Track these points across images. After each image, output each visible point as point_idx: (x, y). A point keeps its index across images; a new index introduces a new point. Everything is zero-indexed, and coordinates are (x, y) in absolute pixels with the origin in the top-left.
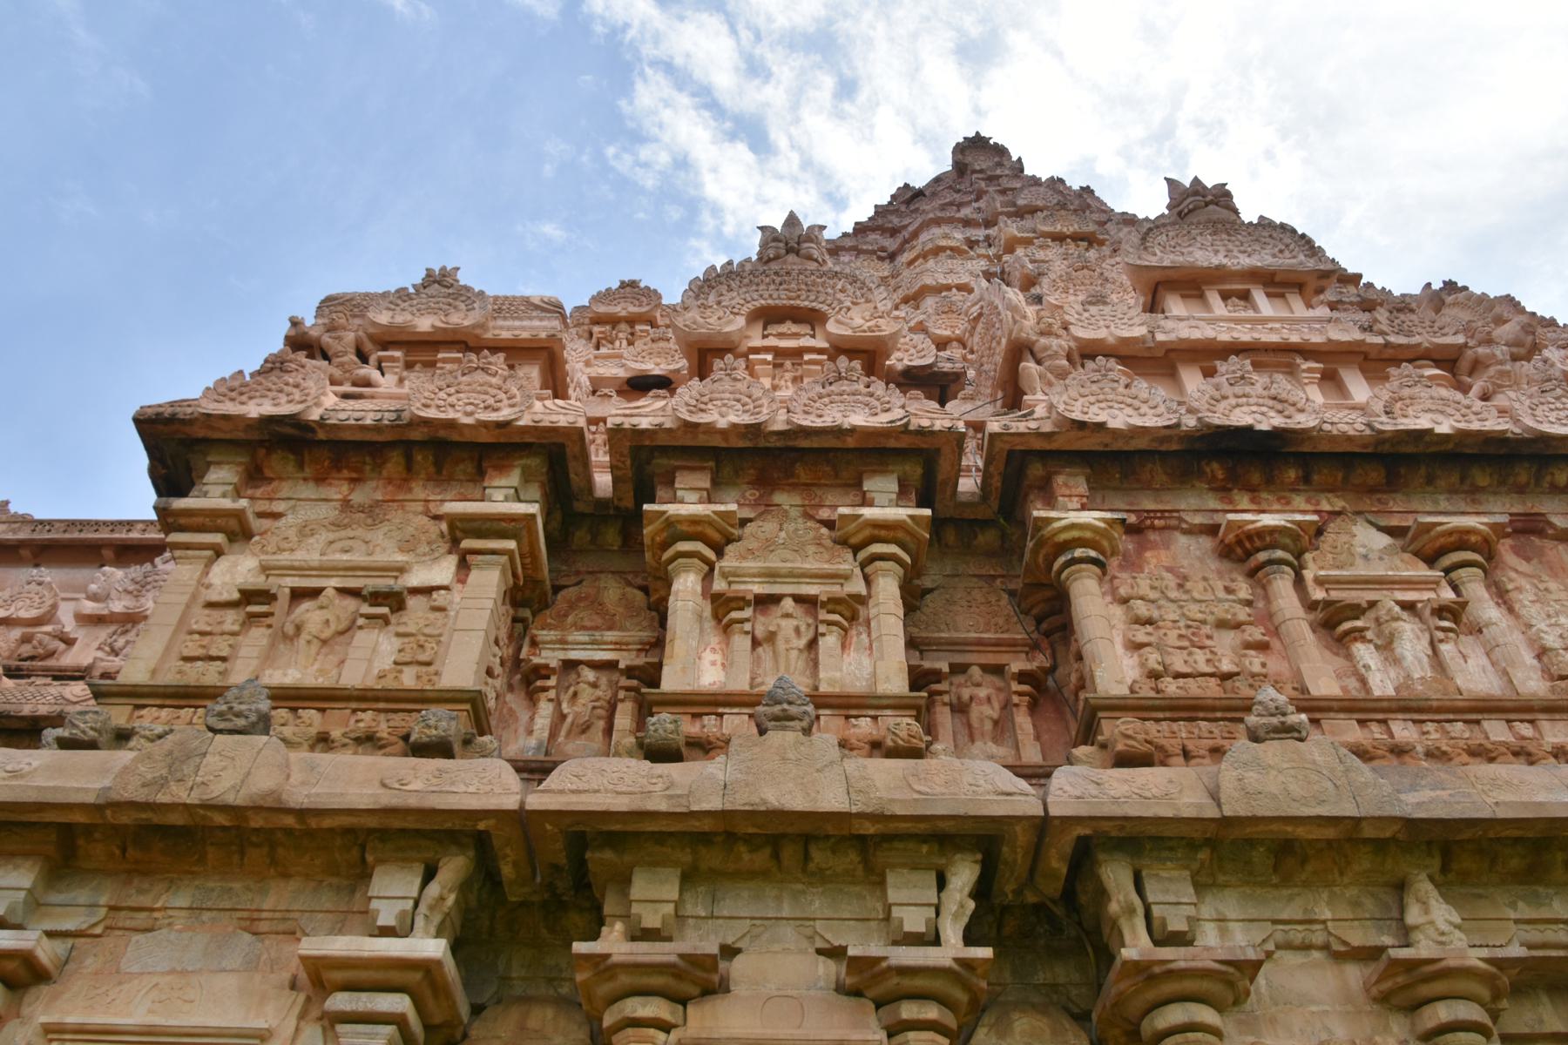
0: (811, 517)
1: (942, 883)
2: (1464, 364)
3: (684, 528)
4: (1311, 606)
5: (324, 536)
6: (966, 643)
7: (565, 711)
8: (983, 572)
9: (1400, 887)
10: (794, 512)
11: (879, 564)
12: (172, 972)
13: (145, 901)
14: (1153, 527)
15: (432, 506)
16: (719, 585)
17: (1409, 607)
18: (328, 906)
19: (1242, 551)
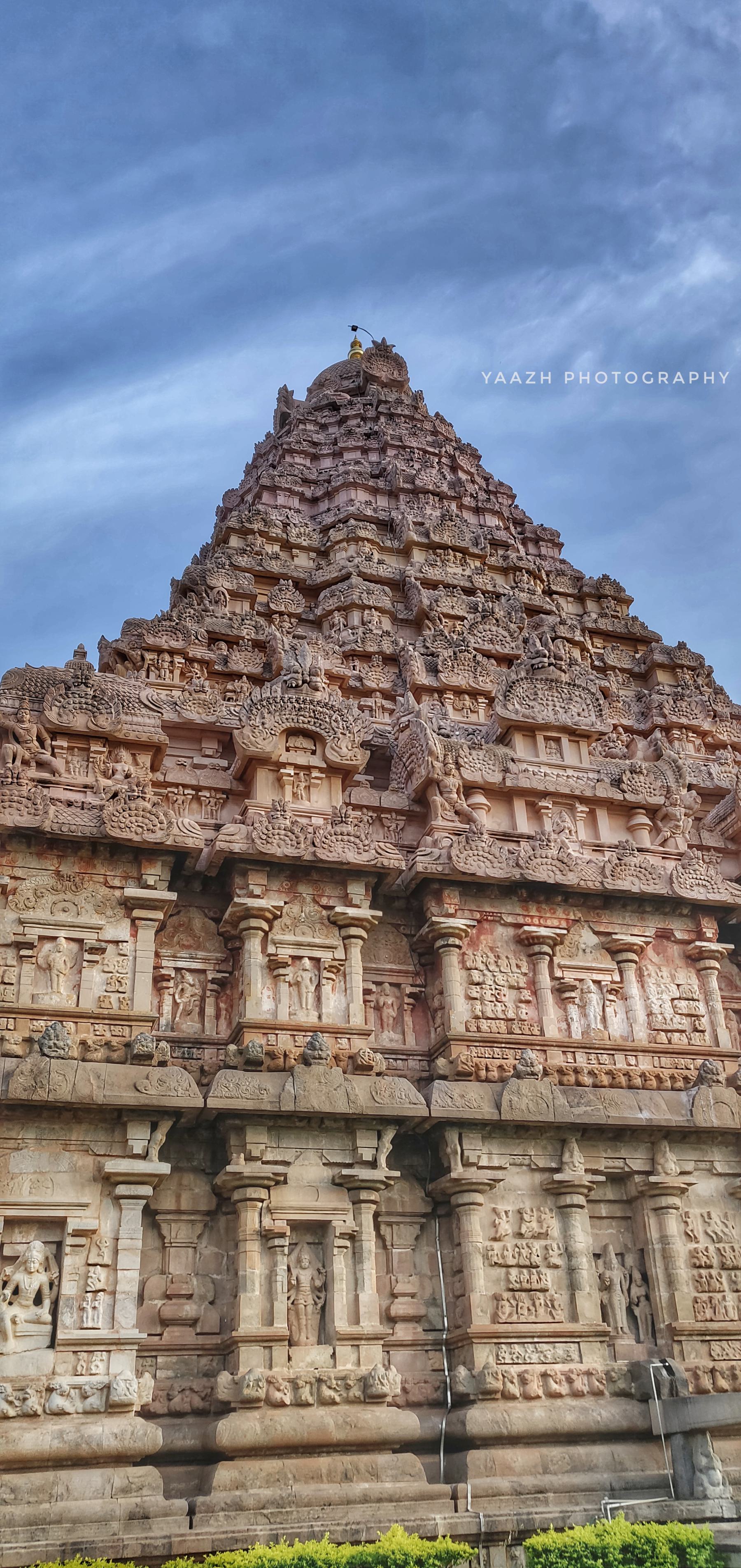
0: (317, 903)
1: (379, 1137)
2: (660, 814)
3: (255, 912)
4: (553, 978)
5: (50, 898)
6: (384, 970)
7: (178, 1001)
8: (394, 921)
9: (564, 1142)
10: (308, 899)
11: (353, 940)
12: (35, 1172)
13: (13, 1134)
14: (487, 920)
15: (109, 878)
16: (271, 949)
17: (597, 982)
18: (103, 1139)
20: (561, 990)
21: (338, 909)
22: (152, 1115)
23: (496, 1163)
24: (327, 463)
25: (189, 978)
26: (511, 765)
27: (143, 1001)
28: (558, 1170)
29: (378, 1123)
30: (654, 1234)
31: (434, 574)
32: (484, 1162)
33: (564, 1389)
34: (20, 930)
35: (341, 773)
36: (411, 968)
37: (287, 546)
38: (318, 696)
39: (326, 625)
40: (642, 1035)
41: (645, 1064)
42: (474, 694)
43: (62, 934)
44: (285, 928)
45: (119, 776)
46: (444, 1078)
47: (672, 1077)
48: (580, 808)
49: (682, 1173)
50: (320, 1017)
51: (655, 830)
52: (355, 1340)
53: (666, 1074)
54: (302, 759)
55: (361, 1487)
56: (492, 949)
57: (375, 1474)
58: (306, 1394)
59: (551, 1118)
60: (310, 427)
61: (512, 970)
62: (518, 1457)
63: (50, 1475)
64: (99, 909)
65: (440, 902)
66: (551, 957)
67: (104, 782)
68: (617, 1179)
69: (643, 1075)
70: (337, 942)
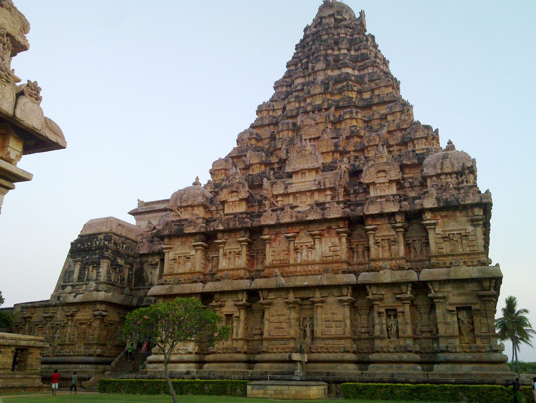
9: (289, 291)
20: (296, 249)
23: (273, 297)
27: (198, 268)
29: (242, 291)
32: (270, 298)
33: (282, 351)
37: (274, 110)
41: (317, 267)
43: (182, 255)
44: (228, 245)
48: (308, 194)
49: (322, 297)
52: (237, 340)
54: (234, 199)
55: (232, 370)
56: (279, 241)
57: (234, 367)
58: (225, 351)
61: (283, 245)
62: (266, 365)
63: (176, 364)
70: (239, 246)
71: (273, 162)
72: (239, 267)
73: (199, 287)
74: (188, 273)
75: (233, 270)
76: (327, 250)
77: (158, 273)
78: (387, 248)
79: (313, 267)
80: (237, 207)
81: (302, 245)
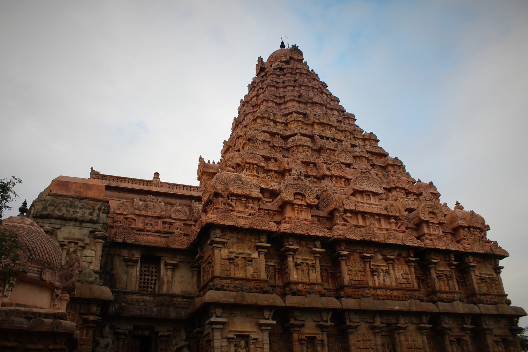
1: (328, 314)
4: (370, 268)
5: (236, 245)
10: (304, 245)
16: (295, 260)
19: (363, 258)
21: (314, 249)
22: (270, 308)
23: (357, 321)
24: (281, 90)
25: (271, 268)
26: (357, 204)
27: (263, 275)
28: (374, 323)
30: (398, 340)
31: (322, 134)
32: (354, 321)
34: (229, 254)
35: (310, 206)
36: (330, 265)
37: (275, 122)
38: (303, 183)
39: (291, 151)
40: (394, 284)
41: (395, 293)
42: (341, 177)
43: (240, 256)
44: (299, 254)
45: (250, 208)
46: (343, 297)
47: (402, 297)
49: (406, 323)
50: (309, 280)
51: (396, 223)
53: (400, 296)
54: (300, 202)
56: (354, 260)
59: (373, 309)
60: (274, 76)
61: (359, 266)
64: (249, 249)
65: (340, 246)
66: (370, 262)
67: (247, 210)
68: (389, 325)
69: (395, 296)
70: (313, 259)
71: (311, 174)
72: (315, 282)
73: (276, 300)
74: (253, 280)
75: (310, 284)
76: (401, 278)
77: (138, 274)
78: (446, 282)
79: (392, 292)
80: (303, 212)
81: (378, 268)
